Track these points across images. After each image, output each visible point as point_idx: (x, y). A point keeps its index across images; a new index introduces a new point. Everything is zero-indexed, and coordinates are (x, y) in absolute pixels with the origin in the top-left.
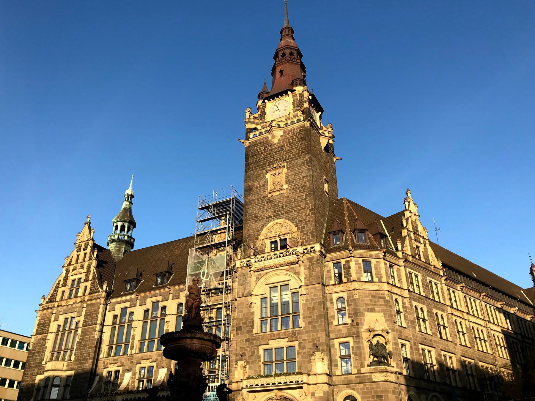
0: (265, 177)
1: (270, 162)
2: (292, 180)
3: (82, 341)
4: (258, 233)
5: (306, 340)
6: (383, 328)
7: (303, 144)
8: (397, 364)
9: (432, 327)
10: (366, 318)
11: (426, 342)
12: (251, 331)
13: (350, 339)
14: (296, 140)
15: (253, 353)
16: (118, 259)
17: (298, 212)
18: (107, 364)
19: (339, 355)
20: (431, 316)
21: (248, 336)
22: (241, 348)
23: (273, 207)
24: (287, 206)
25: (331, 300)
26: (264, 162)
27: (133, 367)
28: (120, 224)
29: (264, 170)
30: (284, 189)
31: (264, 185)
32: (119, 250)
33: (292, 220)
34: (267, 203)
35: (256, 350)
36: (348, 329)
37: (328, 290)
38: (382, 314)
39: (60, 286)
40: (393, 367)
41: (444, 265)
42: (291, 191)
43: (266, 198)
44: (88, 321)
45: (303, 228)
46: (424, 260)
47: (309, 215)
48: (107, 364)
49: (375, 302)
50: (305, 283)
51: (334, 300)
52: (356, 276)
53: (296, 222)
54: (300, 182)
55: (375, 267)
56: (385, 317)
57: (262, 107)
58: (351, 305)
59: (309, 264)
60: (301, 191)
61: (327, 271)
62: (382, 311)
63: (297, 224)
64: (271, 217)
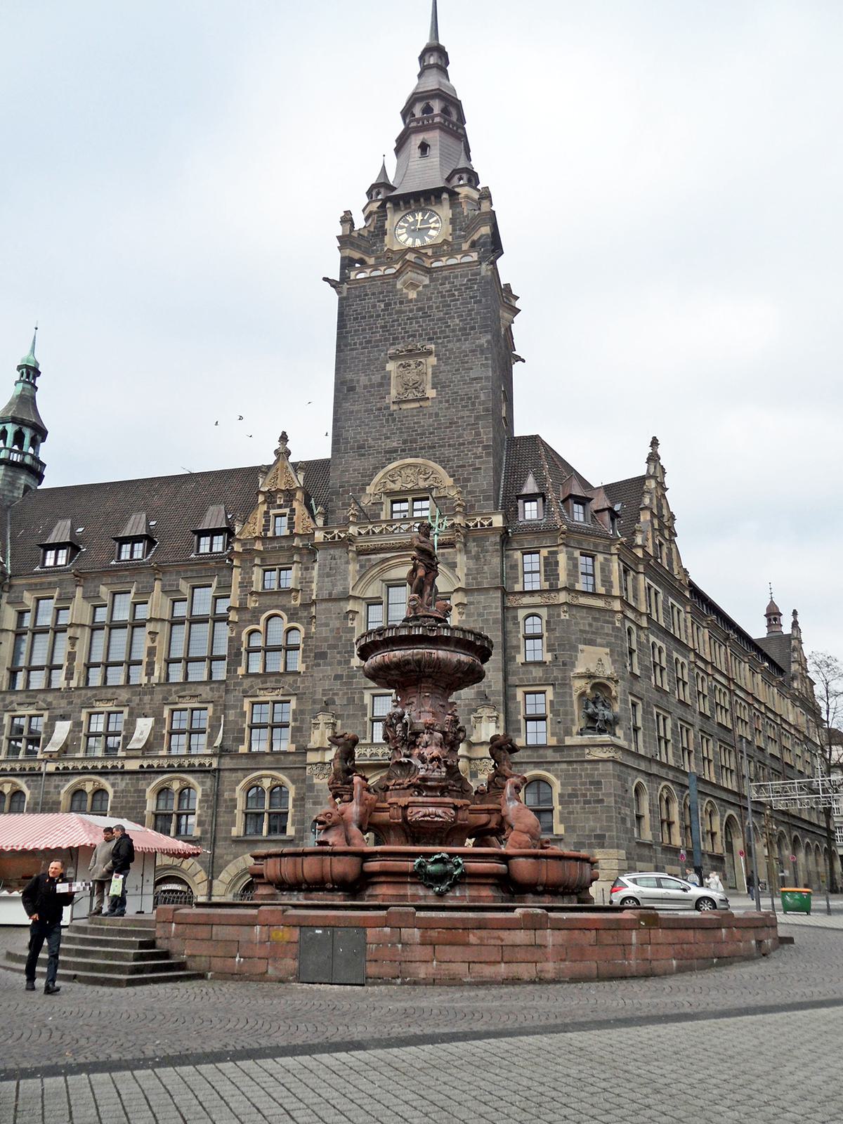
1: (397, 338)
10: (580, 655)
13: (549, 690)
16: (10, 501)
17: (456, 449)
22: (323, 690)
25: (516, 618)
29: (383, 354)
31: (381, 385)
33: (443, 462)
34: (387, 421)
35: (356, 696)
36: (546, 672)
37: (512, 601)
45: (468, 480)
47: (481, 457)
49: (597, 629)
50: (467, 584)
51: (520, 619)
52: (568, 579)
53: (452, 467)
59: (476, 549)
60: (467, 406)
61: (511, 565)
63: (454, 471)
64: (396, 451)
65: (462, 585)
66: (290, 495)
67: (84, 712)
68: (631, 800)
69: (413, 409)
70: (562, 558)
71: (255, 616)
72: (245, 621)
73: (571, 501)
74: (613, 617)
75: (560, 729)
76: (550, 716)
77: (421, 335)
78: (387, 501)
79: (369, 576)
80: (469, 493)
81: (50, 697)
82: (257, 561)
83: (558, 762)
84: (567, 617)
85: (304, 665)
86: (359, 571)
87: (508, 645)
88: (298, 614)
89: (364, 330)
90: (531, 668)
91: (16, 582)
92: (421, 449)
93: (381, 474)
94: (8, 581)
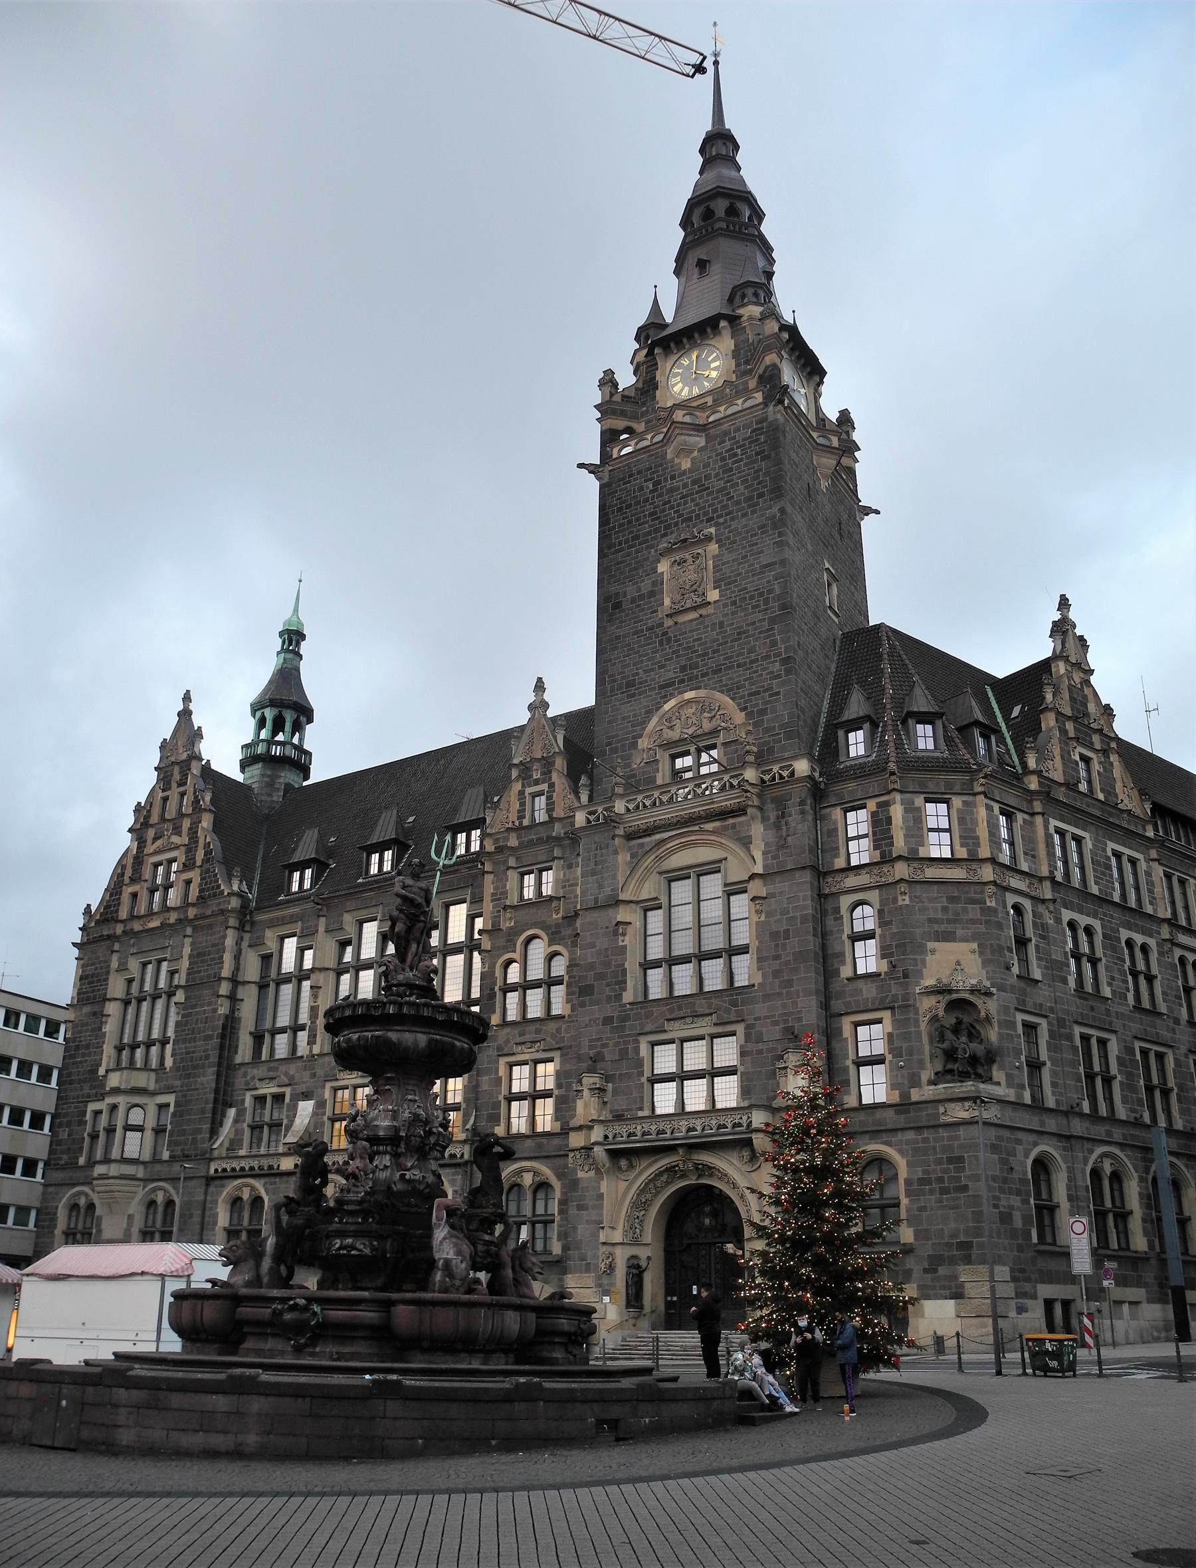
0: (655, 570)
1: (667, 527)
2: (730, 577)
3: (187, 1021)
4: (635, 731)
5: (766, 1017)
6: (974, 982)
7: (761, 470)
8: (1009, 1077)
9: (1113, 978)
10: (929, 959)
11: (1094, 1017)
12: (619, 997)
13: (886, 1015)
14: (741, 460)
15: (624, 1054)
16: (269, 807)
17: (747, 669)
18: (253, 1078)
19: (852, 1056)
20: (1114, 949)
21: (610, 1010)
22: (590, 1041)
23: (678, 657)
24: (717, 651)
25: (837, 910)
26: (650, 526)
27: (316, 1087)
28: (269, 714)
30: (709, 603)
31: (652, 594)
32: (270, 785)
38: (975, 946)
39: (126, 880)
40: (998, 1084)
41: (1159, 811)
42: (731, 608)
43: (659, 631)
44: (199, 972)
45: (763, 712)
46: (1101, 797)
47: (779, 676)
48: (253, 1078)
49: (956, 914)
50: (765, 866)
51: (844, 911)
54: (753, 581)
55: (959, 818)
56: (981, 953)
57: (647, 368)
58: (890, 923)
59: (775, 813)
60: (757, 606)
62: (973, 938)
63: (745, 702)
65: (759, 869)
66: (547, 764)
67: (328, 1085)
68: (1024, 1181)
69: (691, 621)
70: (897, 812)
71: (510, 941)
72: (499, 948)
73: (911, 722)
74: (982, 892)
75: (903, 1076)
76: (889, 1057)
77: (698, 516)
78: (663, 757)
79: (642, 869)
80: (767, 730)
81: (292, 1069)
82: (512, 862)
83: (902, 1129)
84: (907, 902)
85: (569, 1006)
86: (630, 863)
87: (830, 952)
88: (559, 932)
89: (630, 522)
90: (861, 984)
91: (260, 917)
92: (703, 675)
93: (655, 720)
94: (248, 918)
